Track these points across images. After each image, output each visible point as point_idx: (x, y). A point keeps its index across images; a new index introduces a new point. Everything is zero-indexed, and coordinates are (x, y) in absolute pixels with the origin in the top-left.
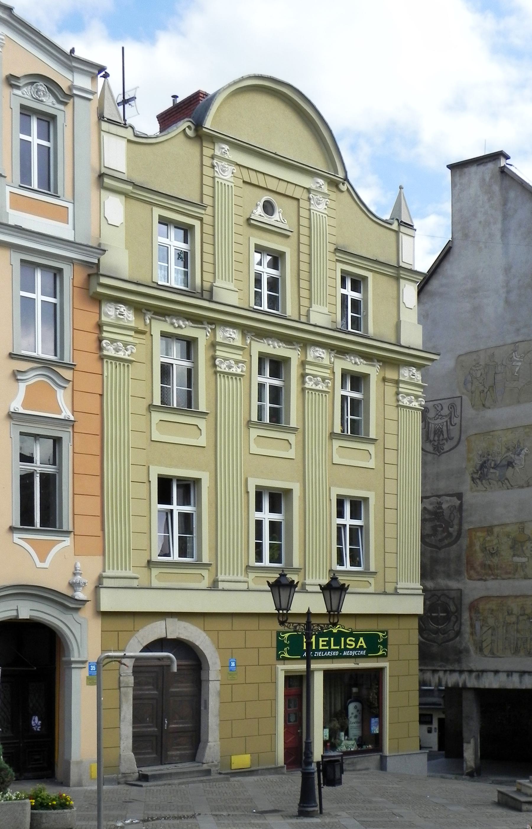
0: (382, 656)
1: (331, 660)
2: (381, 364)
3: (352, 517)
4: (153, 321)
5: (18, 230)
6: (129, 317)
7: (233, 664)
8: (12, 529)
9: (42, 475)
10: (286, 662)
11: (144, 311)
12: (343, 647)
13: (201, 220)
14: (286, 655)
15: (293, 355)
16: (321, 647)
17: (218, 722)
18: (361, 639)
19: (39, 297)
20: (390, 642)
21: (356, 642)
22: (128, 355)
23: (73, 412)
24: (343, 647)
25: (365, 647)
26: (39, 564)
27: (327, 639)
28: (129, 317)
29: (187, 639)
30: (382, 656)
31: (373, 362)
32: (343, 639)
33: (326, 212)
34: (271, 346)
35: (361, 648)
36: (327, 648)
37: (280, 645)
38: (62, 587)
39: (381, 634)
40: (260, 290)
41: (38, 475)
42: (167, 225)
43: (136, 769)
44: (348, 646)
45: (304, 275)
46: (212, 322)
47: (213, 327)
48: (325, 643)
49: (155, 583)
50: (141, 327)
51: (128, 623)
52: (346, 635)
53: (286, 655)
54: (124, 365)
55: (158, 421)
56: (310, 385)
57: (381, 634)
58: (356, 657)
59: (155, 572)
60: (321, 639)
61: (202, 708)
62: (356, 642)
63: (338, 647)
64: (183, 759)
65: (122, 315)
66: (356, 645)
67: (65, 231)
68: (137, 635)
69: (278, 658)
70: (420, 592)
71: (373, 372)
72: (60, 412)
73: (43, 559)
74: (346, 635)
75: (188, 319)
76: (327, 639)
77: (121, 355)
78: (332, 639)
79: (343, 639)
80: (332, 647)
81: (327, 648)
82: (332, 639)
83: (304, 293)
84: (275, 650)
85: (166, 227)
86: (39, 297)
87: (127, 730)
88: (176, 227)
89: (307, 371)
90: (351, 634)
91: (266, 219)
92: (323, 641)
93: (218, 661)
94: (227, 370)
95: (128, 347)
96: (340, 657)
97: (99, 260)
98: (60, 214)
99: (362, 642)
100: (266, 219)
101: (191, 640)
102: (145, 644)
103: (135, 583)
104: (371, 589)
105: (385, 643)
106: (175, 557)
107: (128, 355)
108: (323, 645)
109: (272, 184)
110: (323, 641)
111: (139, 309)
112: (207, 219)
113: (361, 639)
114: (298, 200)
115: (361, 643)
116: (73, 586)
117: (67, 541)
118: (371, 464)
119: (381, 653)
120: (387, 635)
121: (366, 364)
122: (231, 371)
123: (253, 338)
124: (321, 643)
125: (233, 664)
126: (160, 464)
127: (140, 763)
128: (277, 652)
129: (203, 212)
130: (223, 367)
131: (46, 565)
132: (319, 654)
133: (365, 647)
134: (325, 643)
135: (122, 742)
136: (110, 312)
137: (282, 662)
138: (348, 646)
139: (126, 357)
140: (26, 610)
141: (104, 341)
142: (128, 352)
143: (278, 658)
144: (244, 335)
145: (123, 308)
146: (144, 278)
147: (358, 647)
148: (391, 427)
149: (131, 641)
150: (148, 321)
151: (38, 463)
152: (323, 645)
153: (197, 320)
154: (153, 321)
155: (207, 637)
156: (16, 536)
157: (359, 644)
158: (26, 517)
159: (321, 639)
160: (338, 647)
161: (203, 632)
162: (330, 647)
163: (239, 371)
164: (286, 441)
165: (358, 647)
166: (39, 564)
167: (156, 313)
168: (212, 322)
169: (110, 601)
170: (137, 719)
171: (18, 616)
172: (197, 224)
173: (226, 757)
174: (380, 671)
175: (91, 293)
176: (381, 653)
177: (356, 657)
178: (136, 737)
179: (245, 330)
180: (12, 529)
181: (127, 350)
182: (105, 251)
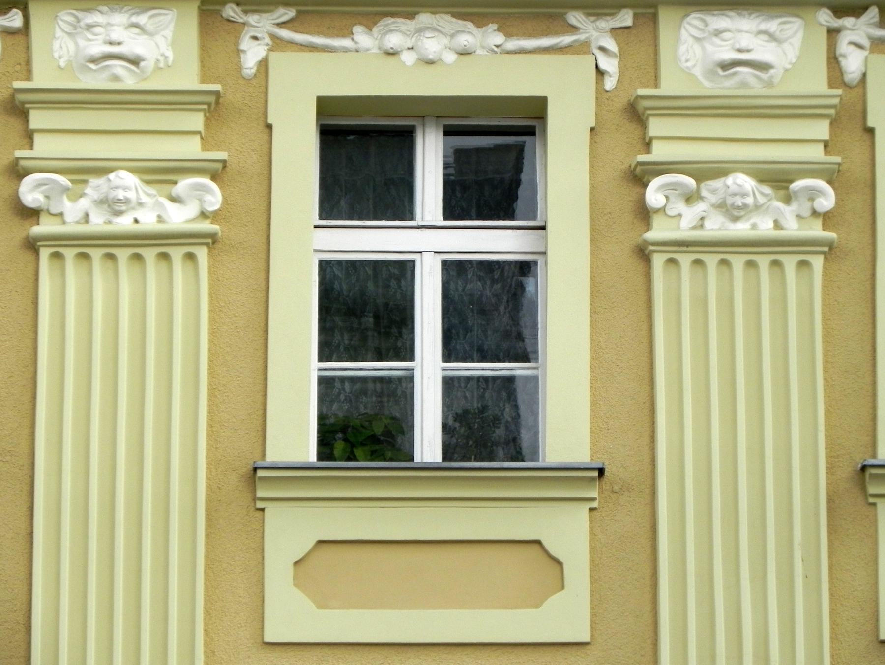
15: (563, 79)
34: (409, 58)
56: (685, 223)
89: (660, 152)
94: (99, 223)
122: (124, 223)
123: (285, 33)
130: (77, 212)
163: (179, 218)
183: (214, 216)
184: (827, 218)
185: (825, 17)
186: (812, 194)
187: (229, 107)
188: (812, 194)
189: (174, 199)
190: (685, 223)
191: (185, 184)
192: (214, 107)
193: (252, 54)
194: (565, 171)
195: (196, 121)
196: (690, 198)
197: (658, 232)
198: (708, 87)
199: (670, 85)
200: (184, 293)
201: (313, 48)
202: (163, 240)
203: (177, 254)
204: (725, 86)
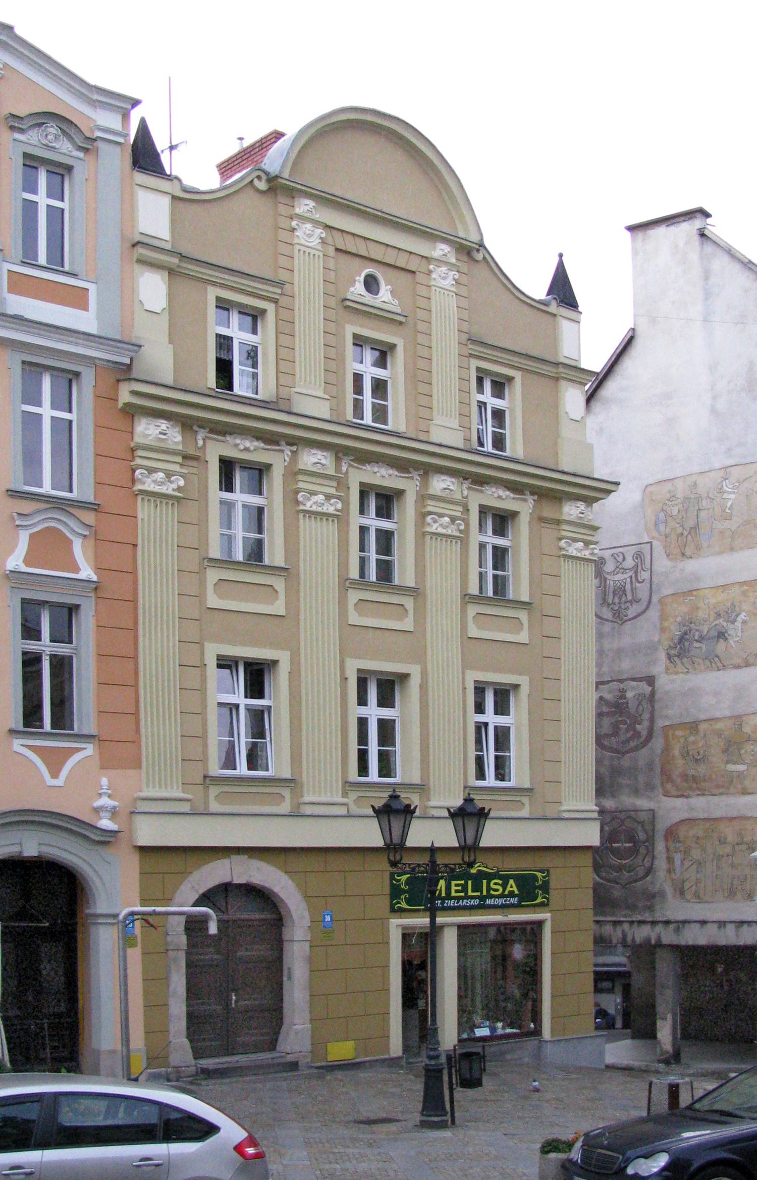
0: (542, 905)
1: (468, 912)
2: (536, 497)
3: (496, 713)
4: (207, 441)
5: (19, 320)
6: (175, 437)
7: (328, 918)
8: (13, 732)
9: (53, 657)
10: (404, 914)
11: (195, 428)
12: (485, 893)
13: (276, 301)
14: (404, 905)
15: (409, 485)
16: (453, 894)
17: (308, 998)
18: (511, 882)
19: (47, 412)
20: (552, 884)
21: (504, 886)
22: (173, 490)
23: (98, 569)
24: (485, 893)
25: (516, 892)
26: (51, 782)
27: (462, 882)
28: (175, 437)
29: (261, 883)
30: (542, 905)
31: (524, 494)
32: (485, 882)
33: (453, 289)
34: (378, 474)
35: (511, 894)
36: (462, 894)
37: (395, 892)
39: (539, 874)
40: (361, 398)
41: (48, 658)
42: (228, 310)
43: (193, 1062)
44: (492, 892)
46: (292, 441)
47: (294, 448)
48: (460, 888)
49: (215, 807)
50: (192, 451)
51: (178, 862)
52: (489, 877)
53: (404, 905)
54: (167, 503)
55: (215, 581)
56: (434, 527)
57: (539, 874)
58: (503, 906)
59: (214, 791)
60: (453, 883)
61: (285, 979)
62: (504, 886)
63: (478, 894)
64: (257, 1048)
65: (165, 434)
66: (504, 890)
67: (84, 320)
68: (191, 878)
70: (596, 815)
71: (525, 507)
72: (77, 570)
73: (55, 775)
74: (489, 877)
75: (258, 439)
76: (462, 882)
77: (163, 489)
78: (470, 882)
79: (485, 882)
80: (470, 893)
81: (462, 894)
82: (470, 882)
84: (388, 897)
85: (226, 312)
86: (47, 412)
87: (178, 1008)
88: (240, 313)
91: (368, 298)
92: (456, 885)
93: (306, 914)
94: (314, 508)
95: (173, 478)
96: (482, 907)
97: (131, 359)
98: (78, 299)
99: (512, 886)
100: (368, 298)
101: (267, 885)
102: (201, 891)
103: (186, 807)
104: (525, 813)
105: (545, 887)
106: (242, 769)
107: (173, 490)
108: (457, 891)
110: (456, 885)
112: (283, 301)
113: (511, 882)
114: (414, 272)
115: (511, 887)
117: (89, 750)
118: (523, 637)
119: (539, 900)
120: (548, 875)
121: (514, 498)
124: (454, 888)
125: (328, 918)
126: (219, 640)
127: (198, 1054)
128: (391, 901)
129: (279, 291)
131: (60, 782)
132: (451, 903)
133: (516, 892)
134: (460, 888)
135: (171, 1026)
136: (148, 430)
137: (399, 914)
138: (492, 892)
139: (170, 492)
140: (31, 845)
141: (138, 472)
142: (175, 486)
144: (338, 460)
145: (164, 425)
147: (506, 893)
149: (182, 887)
150: (200, 443)
151: (48, 640)
152: (457, 891)
153: (271, 440)
154: (207, 441)
155: (290, 882)
156: (18, 744)
157: (508, 889)
158: (32, 714)
159: (453, 883)
160: (478, 894)
161: (283, 874)
162: (466, 893)
163: (331, 510)
164: (401, 608)
165: (506, 893)
166: (51, 782)
167: (211, 431)
168: (292, 441)
169: (149, 833)
170: (192, 992)
171: (21, 852)
172: (270, 307)
175: (120, 405)
176: (539, 900)
177: (503, 906)
178: (192, 1017)
179: (339, 452)
180: (13, 732)
181: (171, 482)
182: (140, 346)
183: (338, 511)
184: (461, 531)
185: (461, 479)
186: (459, 525)
187: (341, 483)
188: (459, 525)
189: (331, 505)
190: (434, 527)
191: (333, 501)
192: (338, 480)
193: (344, 469)
195: (335, 484)
196: (435, 522)
197: (428, 529)
198: (439, 493)
199: (431, 491)
200: (330, 529)
201: (357, 468)
202: (327, 515)
203: (330, 519)
204: (443, 494)
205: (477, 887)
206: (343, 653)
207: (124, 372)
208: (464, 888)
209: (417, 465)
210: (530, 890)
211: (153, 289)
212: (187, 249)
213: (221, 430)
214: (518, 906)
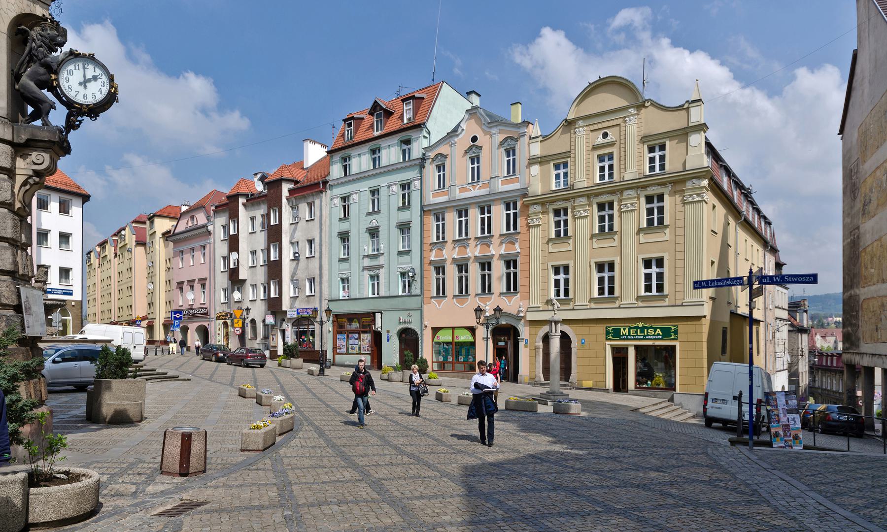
0: (674, 339)
15: (615, 198)
21: (655, 331)
35: (658, 335)
37: (608, 333)
38: (515, 313)
45: (622, 158)
46: (573, 198)
52: (648, 328)
58: (655, 339)
62: (655, 331)
69: (607, 339)
71: (666, 191)
74: (648, 328)
83: (622, 167)
90: (651, 327)
104: (666, 304)
105: (676, 332)
109: (600, 126)
111: (543, 204)
116: (519, 312)
143: (607, 339)
146: (547, 191)
148: (680, 216)
153: (566, 200)
168: (573, 198)
169: (531, 317)
173: (580, 381)
174: (674, 347)
194: (616, 206)
205: (642, 331)
206: (639, 253)
207: (525, 195)
208: (636, 332)
209: (618, 190)
210: (666, 333)
211: (536, 169)
212: (545, 154)
213: (552, 202)
214: (662, 339)
